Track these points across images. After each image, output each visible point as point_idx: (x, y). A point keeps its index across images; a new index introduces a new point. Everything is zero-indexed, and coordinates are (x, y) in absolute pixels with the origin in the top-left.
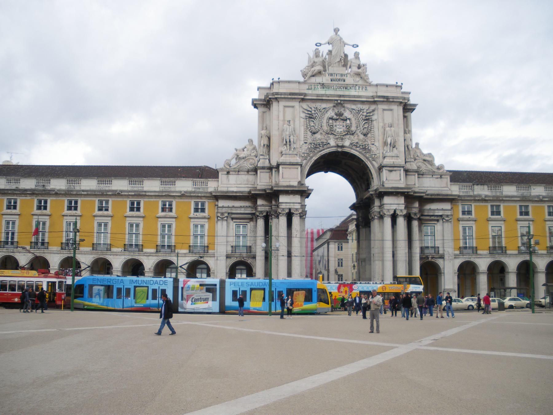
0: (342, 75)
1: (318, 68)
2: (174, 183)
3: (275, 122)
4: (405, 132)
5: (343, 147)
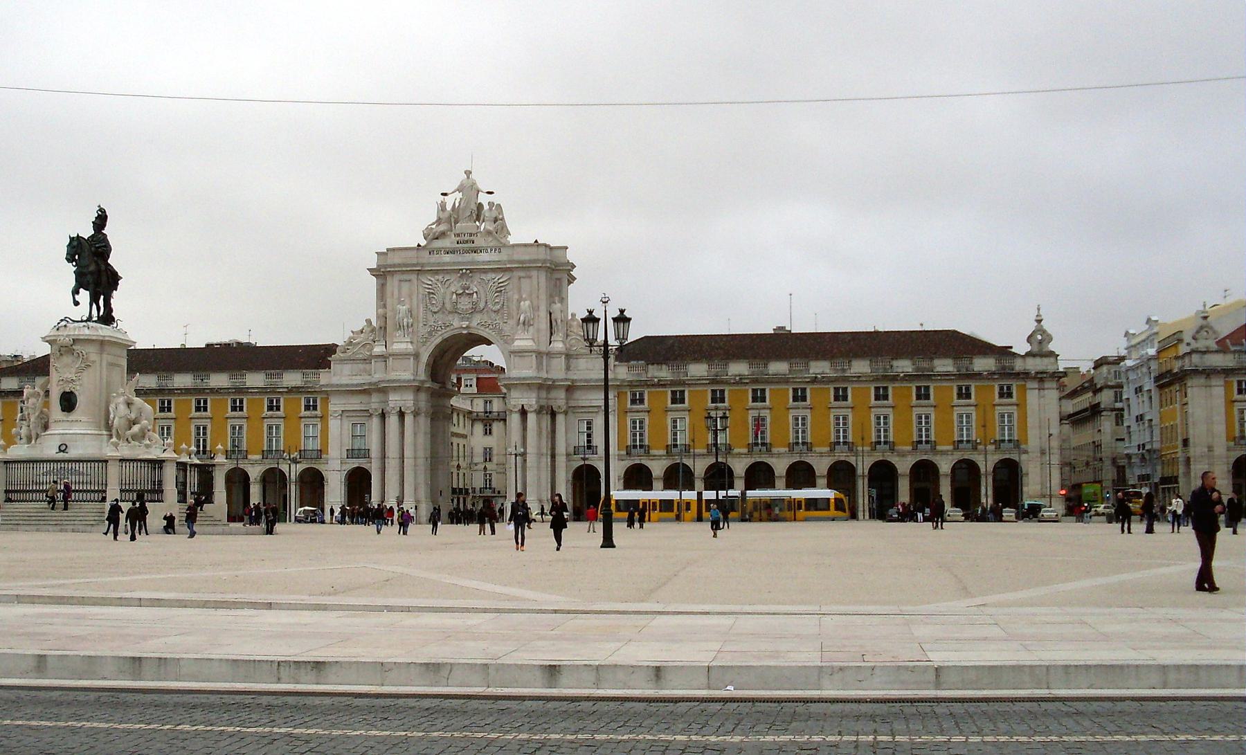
0: (471, 235)
1: (442, 228)
2: (280, 376)
3: (389, 301)
4: (551, 302)
5: (468, 327)
